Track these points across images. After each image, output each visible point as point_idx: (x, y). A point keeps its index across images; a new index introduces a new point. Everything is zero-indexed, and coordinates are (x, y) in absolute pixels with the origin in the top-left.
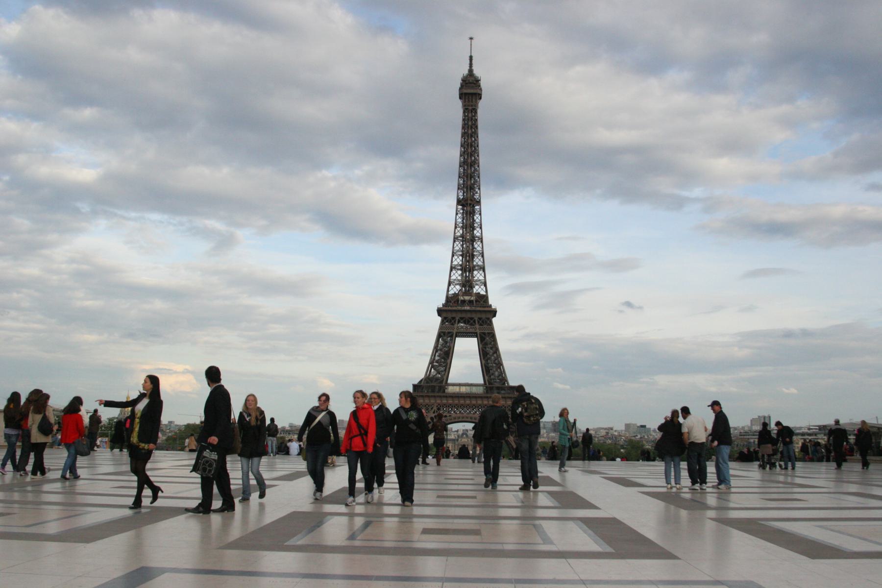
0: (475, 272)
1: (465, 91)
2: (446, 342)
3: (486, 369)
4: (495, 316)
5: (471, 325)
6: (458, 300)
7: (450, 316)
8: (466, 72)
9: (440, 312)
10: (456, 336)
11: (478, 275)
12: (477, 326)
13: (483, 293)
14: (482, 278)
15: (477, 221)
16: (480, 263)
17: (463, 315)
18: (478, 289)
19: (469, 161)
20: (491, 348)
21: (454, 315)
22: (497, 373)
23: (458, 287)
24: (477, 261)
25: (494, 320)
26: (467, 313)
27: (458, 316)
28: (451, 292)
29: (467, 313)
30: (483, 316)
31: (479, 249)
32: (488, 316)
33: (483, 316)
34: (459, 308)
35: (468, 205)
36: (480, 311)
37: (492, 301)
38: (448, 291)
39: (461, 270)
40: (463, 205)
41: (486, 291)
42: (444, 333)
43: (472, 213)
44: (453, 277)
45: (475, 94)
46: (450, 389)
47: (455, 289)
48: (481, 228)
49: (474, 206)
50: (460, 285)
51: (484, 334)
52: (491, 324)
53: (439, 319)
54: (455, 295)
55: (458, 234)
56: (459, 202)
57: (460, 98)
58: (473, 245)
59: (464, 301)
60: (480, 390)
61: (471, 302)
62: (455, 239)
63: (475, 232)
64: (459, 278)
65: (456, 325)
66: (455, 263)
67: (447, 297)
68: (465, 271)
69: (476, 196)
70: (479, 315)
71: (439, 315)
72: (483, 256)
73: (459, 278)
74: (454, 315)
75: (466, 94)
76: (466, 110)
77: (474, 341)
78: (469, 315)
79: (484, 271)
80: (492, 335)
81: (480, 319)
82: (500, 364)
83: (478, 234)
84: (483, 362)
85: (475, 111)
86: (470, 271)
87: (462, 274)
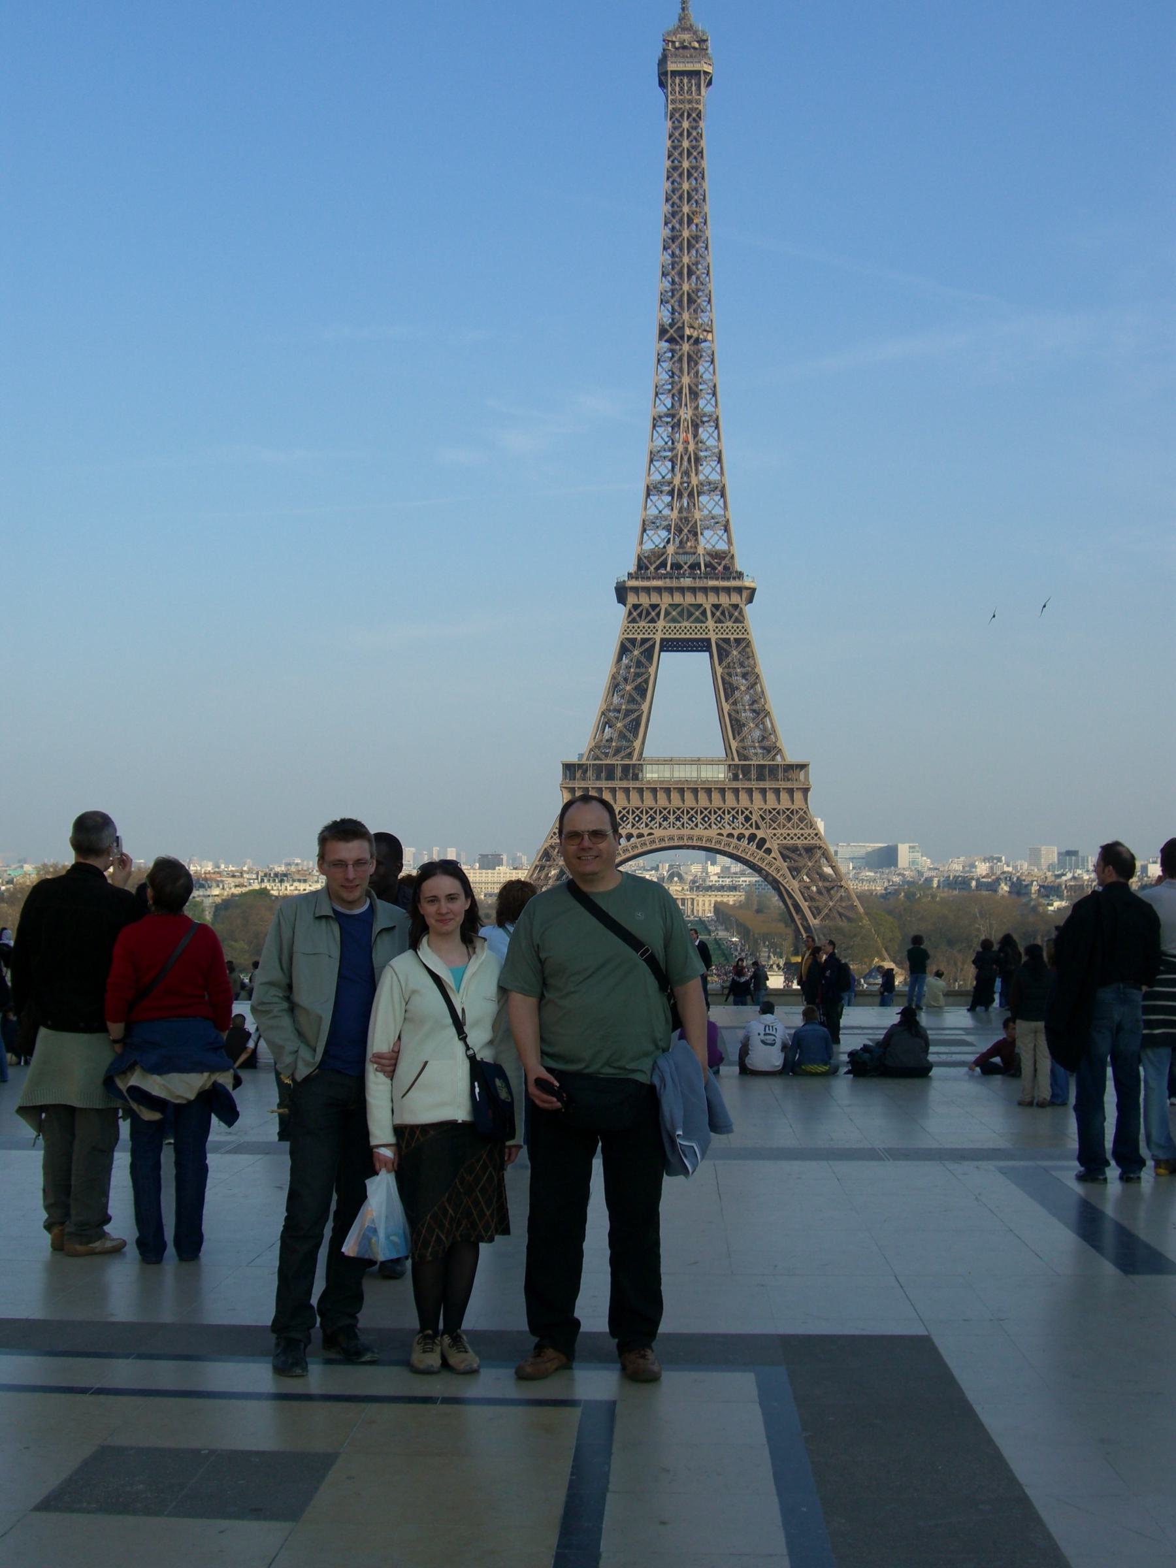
0: (704, 499)
1: (671, 67)
2: (639, 664)
3: (734, 725)
4: (750, 600)
5: (697, 620)
6: (663, 565)
7: (644, 600)
8: (672, 23)
9: (622, 592)
10: (661, 650)
11: (708, 504)
12: (710, 623)
13: (722, 546)
14: (718, 511)
15: (706, 376)
16: (714, 477)
17: (678, 599)
18: (711, 540)
19: (686, 234)
20: (744, 676)
21: (655, 599)
22: (757, 734)
23: (664, 534)
24: (708, 471)
25: (750, 611)
26: (684, 595)
27: (665, 601)
28: (648, 546)
29: (684, 595)
30: (724, 600)
31: (711, 442)
32: (735, 598)
33: (724, 600)
34: (668, 583)
35: (683, 343)
36: (716, 590)
37: (739, 566)
38: (641, 543)
39: (671, 493)
40: (671, 340)
41: (730, 542)
42: (633, 641)
43: (693, 360)
44: (653, 511)
45: (697, 73)
46: (651, 774)
47: (656, 539)
48: (714, 394)
49: (697, 341)
50: (668, 528)
51: (727, 641)
52: (740, 620)
53: (621, 611)
54: (660, 554)
55: (662, 409)
56: (663, 332)
57: (662, 85)
58: (695, 435)
59: (677, 566)
60: (719, 774)
61: (695, 566)
62: (656, 422)
63: (702, 403)
64: (666, 512)
65: (661, 623)
66: (657, 477)
67: (639, 559)
68: (680, 495)
69: (704, 318)
70: (713, 599)
71: (622, 599)
72: (720, 461)
73: (666, 512)
74: (655, 599)
75: (675, 73)
76: (675, 116)
77: (701, 660)
78: (689, 599)
79: (723, 495)
80: (744, 644)
81: (716, 607)
82: (761, 713)
83: (709, 409)
84: (726, 707)
85: (696, 117)
86: (691, 495)
87: (670, 506)
